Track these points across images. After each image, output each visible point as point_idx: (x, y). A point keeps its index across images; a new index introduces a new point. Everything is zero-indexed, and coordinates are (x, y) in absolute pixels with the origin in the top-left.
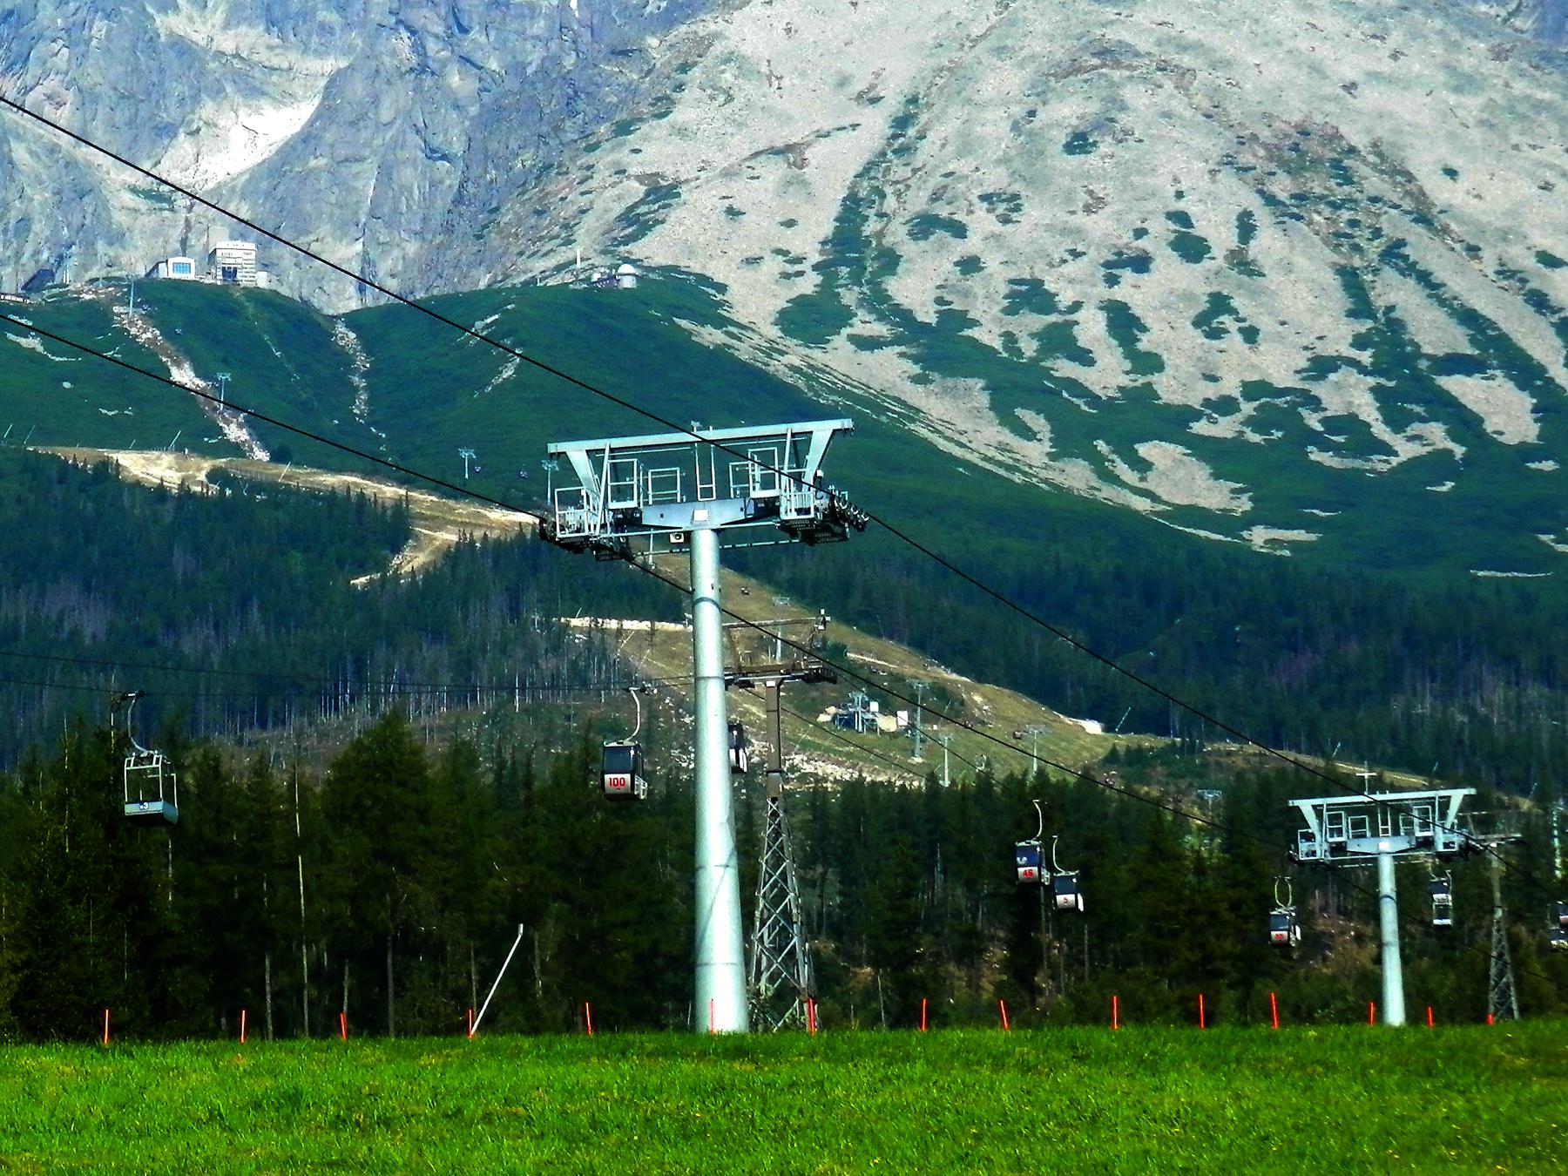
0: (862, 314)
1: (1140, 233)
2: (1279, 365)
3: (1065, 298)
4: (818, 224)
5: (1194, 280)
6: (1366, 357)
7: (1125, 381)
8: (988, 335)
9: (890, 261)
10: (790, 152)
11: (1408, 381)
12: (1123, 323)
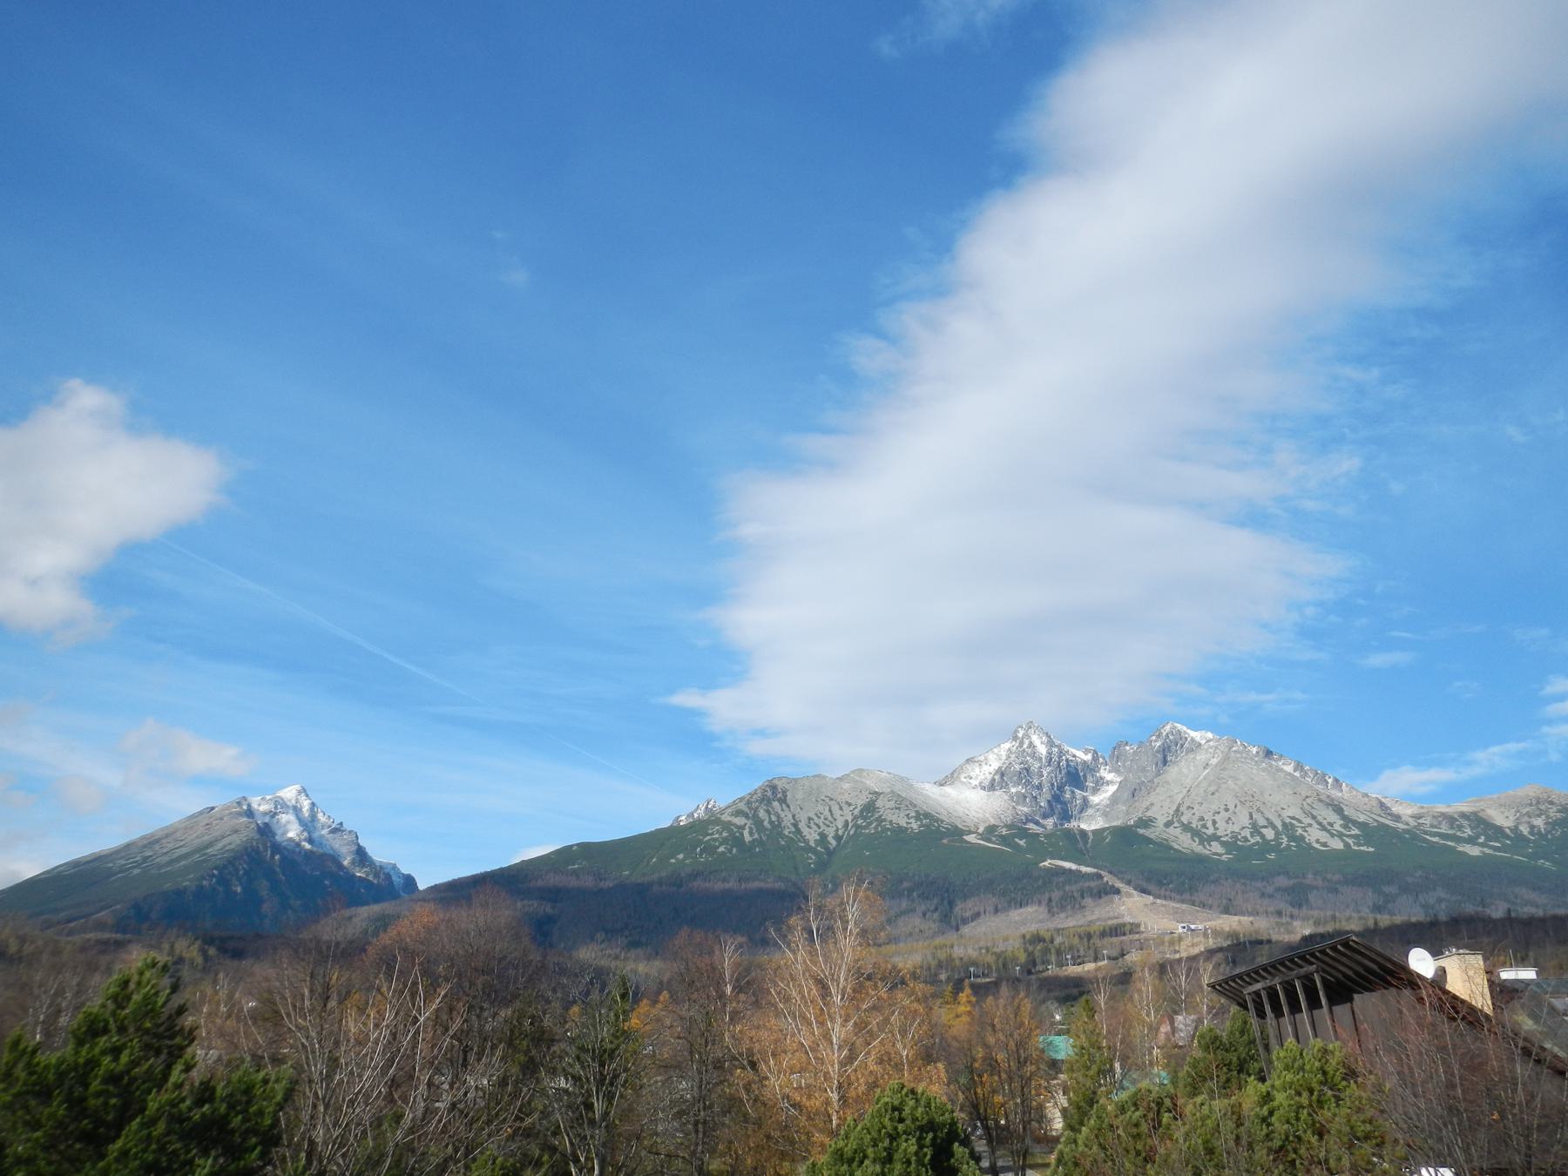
5: (1227, 815)
11: (1256, 829)
12: (1214, 822)
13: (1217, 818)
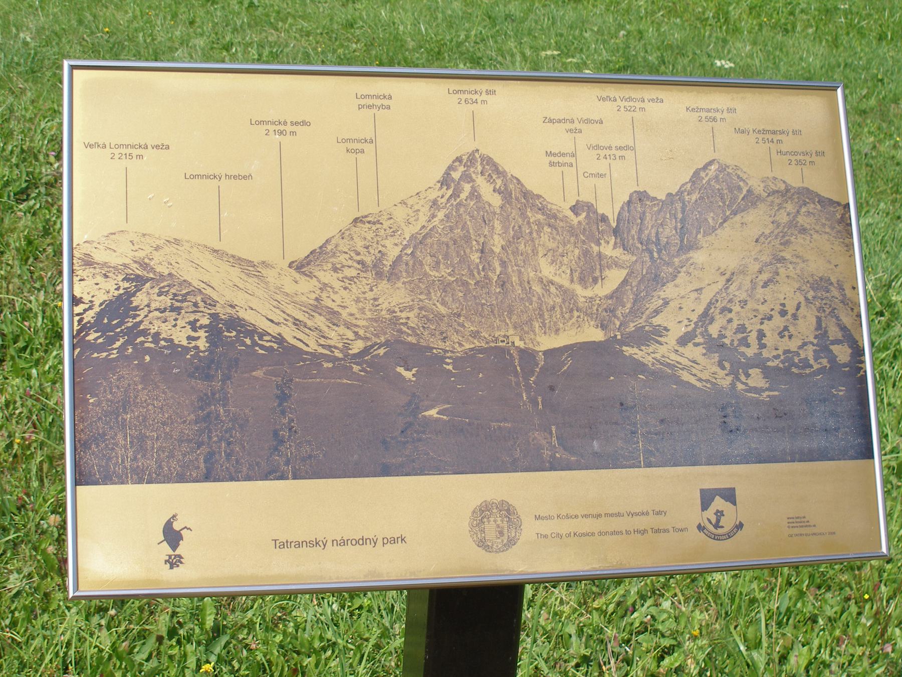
0: (699, 336)
1: (772, 310)
2: (793, 345)
3: (748, 330)
4: (700, 309)
6: (815, 341)
7: (756, 351)
8: (727, 341)
9: (712, 320)
10: (699, 290)
12: (761, 335)
13: (766, 327)
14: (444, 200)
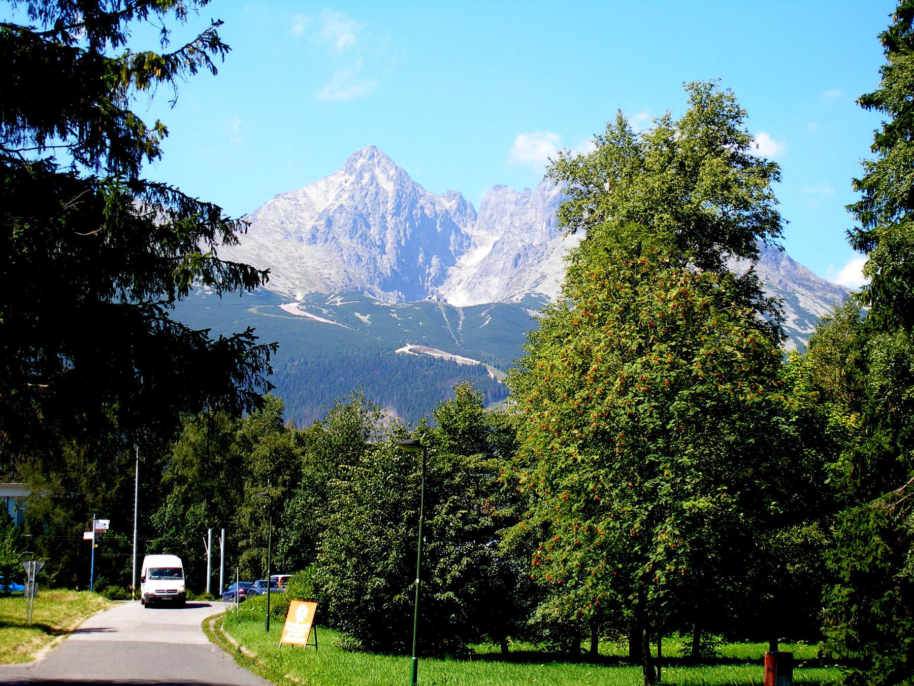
14: (348, 184)
